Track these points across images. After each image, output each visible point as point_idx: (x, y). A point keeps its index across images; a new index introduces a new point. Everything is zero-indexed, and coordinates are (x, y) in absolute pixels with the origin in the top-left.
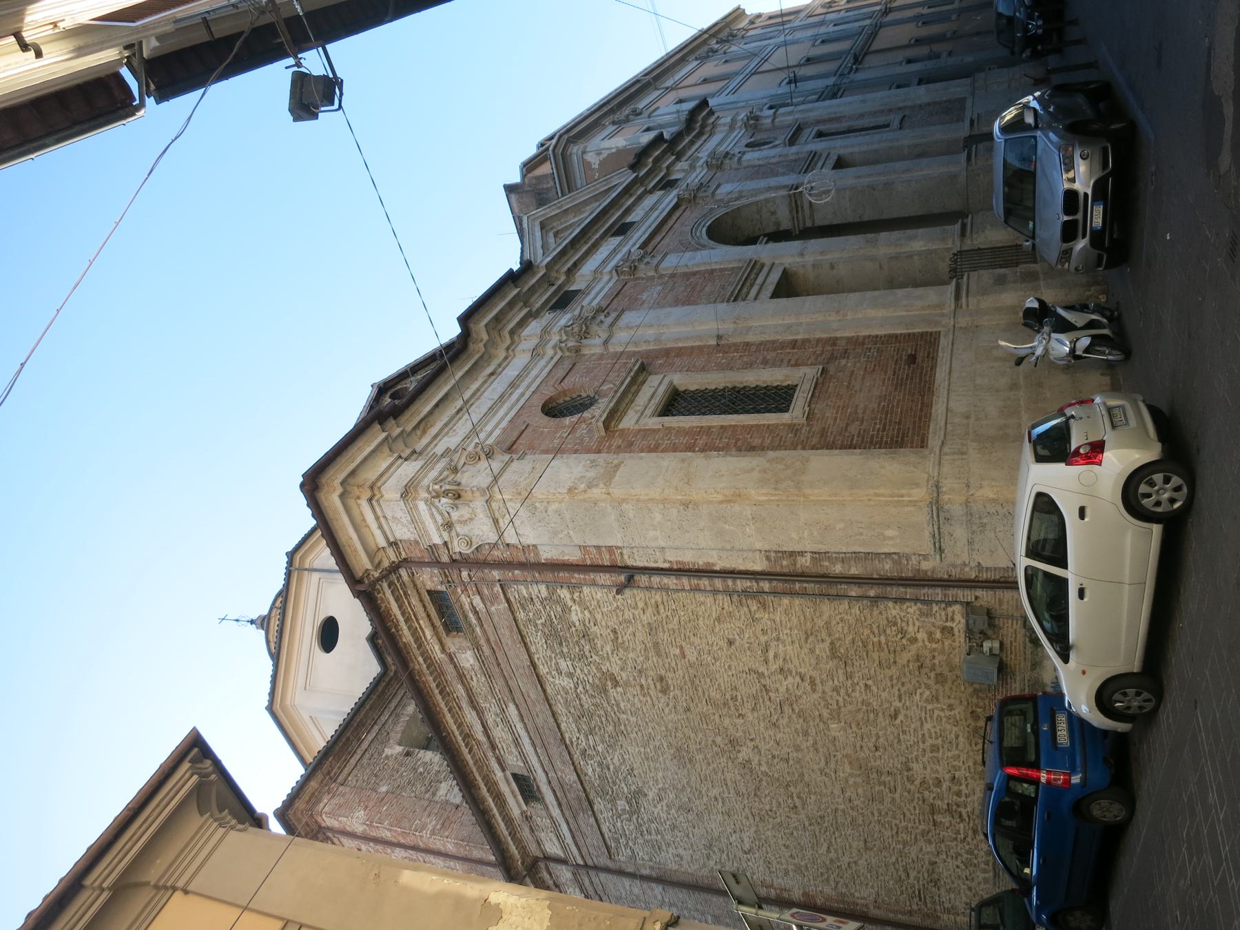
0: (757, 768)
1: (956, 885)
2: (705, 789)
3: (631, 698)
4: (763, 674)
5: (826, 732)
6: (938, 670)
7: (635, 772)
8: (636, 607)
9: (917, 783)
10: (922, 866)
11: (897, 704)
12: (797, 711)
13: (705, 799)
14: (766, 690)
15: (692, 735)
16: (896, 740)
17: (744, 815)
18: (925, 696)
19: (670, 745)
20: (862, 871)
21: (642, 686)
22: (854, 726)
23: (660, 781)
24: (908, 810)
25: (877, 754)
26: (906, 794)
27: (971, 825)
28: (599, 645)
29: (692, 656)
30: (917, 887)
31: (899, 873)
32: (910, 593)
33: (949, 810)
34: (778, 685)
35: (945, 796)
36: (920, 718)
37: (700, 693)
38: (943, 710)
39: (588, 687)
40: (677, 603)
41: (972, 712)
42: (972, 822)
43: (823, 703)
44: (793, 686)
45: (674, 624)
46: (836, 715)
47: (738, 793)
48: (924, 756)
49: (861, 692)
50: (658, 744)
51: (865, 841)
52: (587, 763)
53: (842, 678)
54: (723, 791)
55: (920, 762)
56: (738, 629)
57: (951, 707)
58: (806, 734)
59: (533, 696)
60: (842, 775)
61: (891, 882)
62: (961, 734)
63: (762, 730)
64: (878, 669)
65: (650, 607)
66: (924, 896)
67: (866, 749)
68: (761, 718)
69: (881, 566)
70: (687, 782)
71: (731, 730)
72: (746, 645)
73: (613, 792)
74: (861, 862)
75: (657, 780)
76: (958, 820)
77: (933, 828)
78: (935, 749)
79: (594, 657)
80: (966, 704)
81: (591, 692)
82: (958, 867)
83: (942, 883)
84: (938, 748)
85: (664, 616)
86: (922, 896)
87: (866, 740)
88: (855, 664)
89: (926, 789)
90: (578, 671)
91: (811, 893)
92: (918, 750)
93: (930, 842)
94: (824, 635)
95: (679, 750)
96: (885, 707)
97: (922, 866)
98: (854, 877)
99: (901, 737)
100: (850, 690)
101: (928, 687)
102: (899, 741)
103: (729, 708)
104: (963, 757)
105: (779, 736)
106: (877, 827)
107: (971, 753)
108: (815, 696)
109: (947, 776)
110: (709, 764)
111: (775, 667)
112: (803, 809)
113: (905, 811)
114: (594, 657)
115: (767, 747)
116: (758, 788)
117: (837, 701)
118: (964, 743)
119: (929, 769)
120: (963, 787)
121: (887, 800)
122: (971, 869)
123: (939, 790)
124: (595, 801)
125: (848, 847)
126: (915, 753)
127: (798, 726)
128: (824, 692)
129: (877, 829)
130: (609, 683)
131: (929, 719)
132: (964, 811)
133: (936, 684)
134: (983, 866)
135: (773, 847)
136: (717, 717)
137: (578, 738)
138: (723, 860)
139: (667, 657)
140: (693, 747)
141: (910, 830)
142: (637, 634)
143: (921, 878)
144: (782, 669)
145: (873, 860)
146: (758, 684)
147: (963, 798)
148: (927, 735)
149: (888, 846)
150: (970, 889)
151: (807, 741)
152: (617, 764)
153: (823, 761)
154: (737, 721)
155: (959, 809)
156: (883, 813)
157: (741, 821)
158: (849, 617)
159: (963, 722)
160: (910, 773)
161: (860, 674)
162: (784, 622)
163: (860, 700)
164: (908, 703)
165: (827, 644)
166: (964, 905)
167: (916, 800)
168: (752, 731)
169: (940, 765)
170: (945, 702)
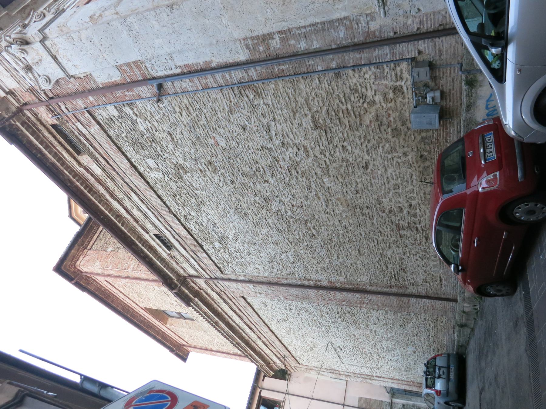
0: (285, 214)
1: (417, 270)
2: (259, 230)
3: (197, 179)
4: (271, 149)
5: (322, 184)
6: (394, 126)
7: (217, 225)
9: (387, 211)
10: (395, 262)
11: (367, 157)
12: (300, 173)
13: (261, 236)
14: (276, 160)
15: (241, 198)
16: (369, 184)
17: (285, 243)
18: (386, 148)
19: (231, 207)
20: (359, 267)
21: (201, 170)
24: (383, 229)
25: (358, 195)
26: (380, 219)
27: (424, 235)
28: (165, 146)
29: (222, 143)
30: (393, 273)
31: (382, 267)
32: (364, 56)
33: (409, 227)
34: (283, 156)
35: (406, 218)
36: (384, 166)
37: (236, 169)
38: (399, 157)
39: (170, 176)
40: (199, 103)
41: (421, 156)
42: (424, 232)
43: (316, 165)
44: (293, 155)
45: (203, 122)
46: (326, 171)
47: (278, 230)
48: (389, 193)
49: (340, 152)
51: (359, 251)
52: (190, 223)
53: (326, 143)
54: (269, 230)
55: (387, 197)
56: (245, 117)
57: (405, 154)
58: (310, 188)
59: (143, 187)
60: (337, 212)
61: (378, 272)
62: (413, 173)
63: (282, 189)
64: (349, 131)
65: (183, 110)
66: (398, 278)
67: (350, 193)
68: (279, 181)
69: (336, 34)
70: (248, 228)
71: (263, 192)
72: (255, 129)
73: (210, 238)
74: (358, 262)
75: (231, 228)
76: (416, 232)
78: (397, 187)
79: (166, 155)
80: (415, 150)
81: (173, 178)
82: (417, 260)
83: (408, 270)
84: (399, 187)
85: (195, 115)
86: (397, 277)
87: (349, 186)
88: (332, 130)
89: (393, 215)
90: (160, 166)
91: (333, 281)
92: (385, 189)
93: (398, 247)
95: (237, 208)
96: (358, 161)
97: (395, 262)
98: (355, 271)
99: (373, 182)
100: (332, 153)
101: (387, 140)
102: (372, 184)
103: (257, 177)
104: (417, 189)
105: (293, 191)
106: (365, 242)
107: (422, 187)
108: (310, 160)
109: (406, 205)
111: (277, 142)
112: (318, 235)
113: (381, 229)
114: (166, 155)
115: (288, 200)
116: (289, 226)
117: (325, 161)
118: (417, 180)
119: (393, 201)
120: (418, 211)
121: (369, 224)
122: (426, 261)
123: (401, 215)
124: (203, 244)
125: (349, 255)
126: (383, 192)
127: (304, 183)
128: (315, 156)
129: (365, 243)
130: (181, 171)
131: (390, 166)
132: (419, 226)
133: (393, 137)
134: (432, 258)
135: (306, 259)
136: (251, 183)
137: (179, 209)
138: (281, 269)
139: (208, 147)
140: (244, 206)
141: (385, 241)
142: (183, 133)
143: (395, 268)
144: (283, 143)
145: (365, 261)
146: (270, 157)
147: (419, 218)
148: (390, 178)
149: (373, 252)
150: (425, 272)
151: (311, 192)
152: (206, 222)
153: (324, 204)
155: (416, 226)
156: (367, 233)
157: (285, 247)
158: (321, 92)
159: (415, 165)
160: (382, 205)
161: (337, 138)
162: (275, 105)
163: (341, 158)
164: (374, 156)
165: (309, 117)
166: (422, 281)
167: (387, 223)
168: (275, 191)
169: (401, 198)
170: (400, 151)
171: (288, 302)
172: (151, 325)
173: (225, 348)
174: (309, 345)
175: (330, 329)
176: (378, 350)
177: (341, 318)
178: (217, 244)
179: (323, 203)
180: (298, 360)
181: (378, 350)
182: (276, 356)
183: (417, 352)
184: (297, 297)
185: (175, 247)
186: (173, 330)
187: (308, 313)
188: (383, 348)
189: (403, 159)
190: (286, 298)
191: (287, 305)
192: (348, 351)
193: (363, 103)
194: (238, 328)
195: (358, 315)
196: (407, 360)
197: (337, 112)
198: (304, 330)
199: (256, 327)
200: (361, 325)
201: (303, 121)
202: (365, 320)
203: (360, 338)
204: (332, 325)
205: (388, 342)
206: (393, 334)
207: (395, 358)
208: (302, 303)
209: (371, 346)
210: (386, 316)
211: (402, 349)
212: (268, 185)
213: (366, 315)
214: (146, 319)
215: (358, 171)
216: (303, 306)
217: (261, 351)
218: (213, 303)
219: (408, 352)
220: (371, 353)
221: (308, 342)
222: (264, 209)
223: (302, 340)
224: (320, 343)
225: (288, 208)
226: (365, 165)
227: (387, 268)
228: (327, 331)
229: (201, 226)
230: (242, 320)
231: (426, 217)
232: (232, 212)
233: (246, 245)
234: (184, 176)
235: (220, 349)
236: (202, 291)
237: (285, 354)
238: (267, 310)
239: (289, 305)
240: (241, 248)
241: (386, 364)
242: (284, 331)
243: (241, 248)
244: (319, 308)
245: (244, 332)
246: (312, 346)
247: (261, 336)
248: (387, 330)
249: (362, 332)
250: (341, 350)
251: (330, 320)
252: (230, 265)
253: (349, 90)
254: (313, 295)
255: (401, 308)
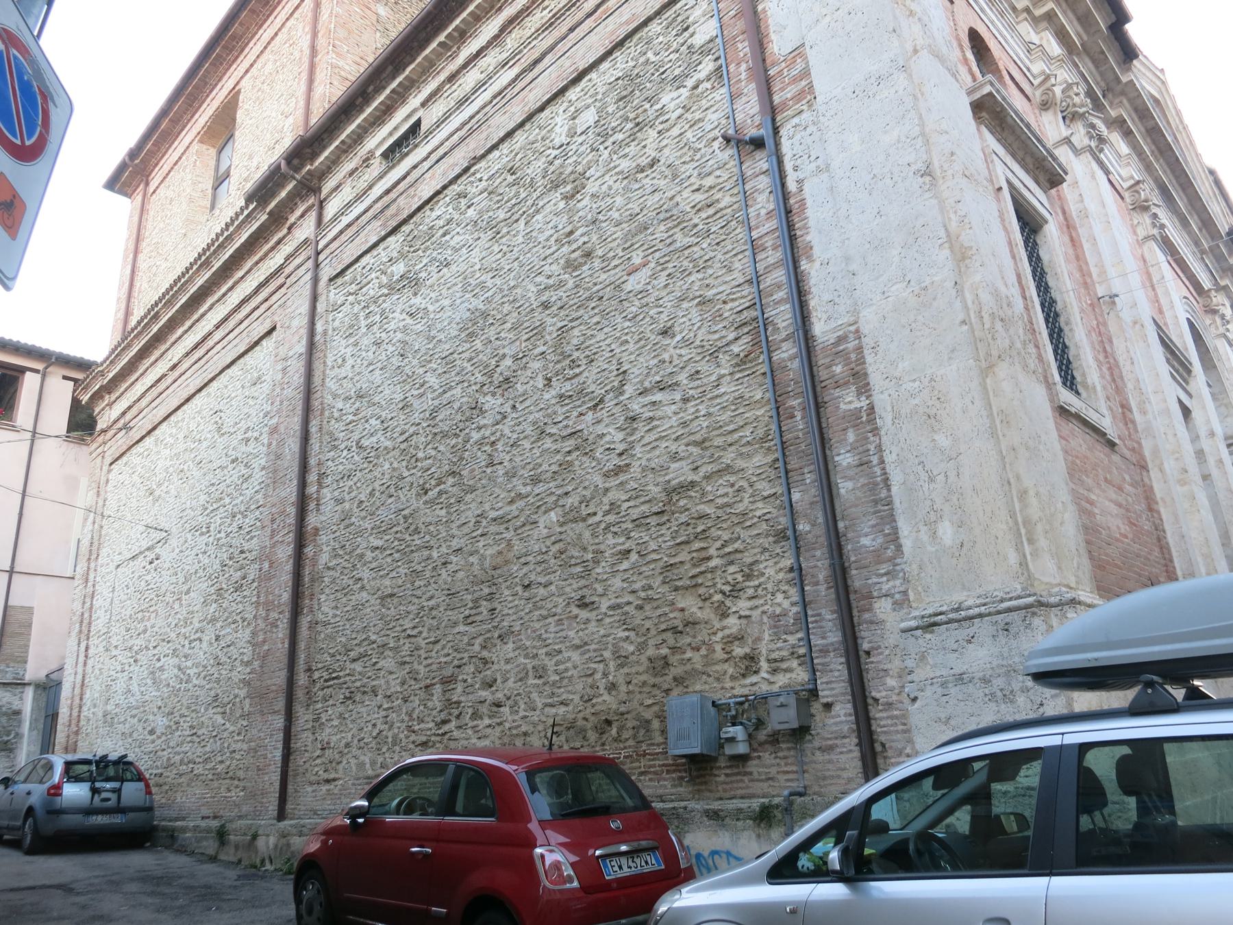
0: (473, 426)
2: (435, 366)
3: (551, 225)
4: (621, 394)
5: (543, 508)
6: (673, 659)
7: (445, 270)
8: (701, 176)
9: (485, 654)
10: (369, 678)
11: (604, 605)
12: (568, 458)
13: (421, 371)
14: (597, 405)
15: (508, 325)
16: (544, 613)
17: (407, 427)
18: (625, 645)
19: (488, 301)
20: (353, 597)
21: (571, 233)
22: (557, 546)
23: (437, 305)
24: (443, 647)
25: (519, 589)
26: (466, 639)
28: (627, 150)
29: (633, 283)
30: (341, 674)
31: (356, 648)
33: (449, 704)
34: (607, 421)
35: (470, 697)
36: (586, 644)
37: (574, 315)
38: (605, 675)
39: (557, 162)
40: (721, 231)
41: (608, 723)
42: (438, 738)
43: (587, 493)
44: (608, 443)
45: (681, 240)
46: (572, 517)
47: (435, 410)
48: (526, 656)
49: (615, 545)
50: (489, 284)
51: (392, 595)
52: (448, 205)
53: (635, 513)
54: (435, 391)
55: (516, 653)
56: (692, 335)
57: (612, 687)
58: (535, 480)
59: (531, 97)
60: (481, 544)
61: (343, 639)
62: (571, 708)
63: (531, 418)
64: (661, 564)
65: (706, 195)
66: (331, 686)
68: (549, 411)
69: (867, 530)
70: (440, 341)
71: (524, 376)
72: (666, 356)
73: (414, 252)
74: (364, 594)
75: (438, 301)
76: (438, 719)
77: (422, 684)
78: (540, 673)
79: (606, 152)
80: (622, 709)
81: (552, 168)
82: (374, 725)
84: (541, 677)
85: (696, 221)
86: (332, 683)
87: (539, 569)
88: (664, 527)
89: (477, 667)
90: (580, 140)
91: (318, 538)
92: (534, 647)
93: (403, 683)
94: (706, 469)
95: (485, 315)
96: (597, 586)
97: (369, 678)
98: (344, 589)
99: (550, 620)
101: (642, 647)
102: (546, 618)
103: (559, 362)
104: (535, 716)
105: (527, 444)
106: (413, 608)
107: (540, 728)
108: (598, 480)
109: (500, 695)
110: (470, 359)
111: (636, 407)
112: (426, 503)
114: (606, 152)
115: (507, 431)
116: (445, 435)
117: (595, 514)
118: (557, 714)
119: (508, 667)
120: (487, 721)
121: (454, 615)
122: (373, 745)
123: (477, 686)
124: (399, 235)
125: (381, 573)
126: (528, 643)
127: (545, 467)
128: (607, 490)
129: (411, 608)
130: (569, 188)
131: (587, 656)
133: (650, 659)
134: (380, 759)
135: (369, 476)
136: (543, 349)
137: (480, 180)
138: (344, 418)
139: (624, 249)
140: (491, 333)
141: (416, 652)
142: (656, 194)
143: (353, 678)
144: (633, 419)
145: (369, 610)
146: (603, 391)
148: (560, 657)
149: (391, 626)
150: (347, 745)
151: (525, 485)
152: (452, 243)
153: (497, 513)
154: (540, 377)
155: (453, 719)
156: (434, 613)
157: (396, 427)
158: (746, 501)
159: (590, 710)
161: (647, 538)
162: (718, 401)
163: (602, 547)
164: (608, 620)
165: (691, 477)
166: (326, 740)
167: (459, 656)
168: (527, 403)
169: (515, 682)
171: (265, 436)
172: (196, 104)
173: (145, 285)
174: (160, 485)
175: (202, 534)
176: (155, 647)
177: (231, 559)
178: (399, 269)
179: (500, 512)
180: (119, 462)
181: (155, 647)
182: (130, 408)
183: (154, 736)
184: (278, 457)
185: (391, 168)
186: (184, 158)
187: (239, 482)
188: (159, 660)
189: (602, 684)
190: (274, 430)
191: (256, 434)
192: (148, 578)
193: (723, 593)
194: (195, 317)
195: (239, 599)
196: (133, 716)
197: (703, 535)
198: (197, 473)
199: (200, 359)
200: (214, 605)
201: (683, 463)
202: (226, 614)
203: (181, 605)
204: (211, 539)
205: (176, 671)
206: (195, 681)
207: (135, 688)
208: (263, 468)
209: (163, 630)
210: (237, 663)
211: (159, 703)
212: (541, 386)
213: (238, 618)
214: (211, 92)
215: (575, 586)
216: (256, 470)
217: (141, 371)
218: (256, 258)
219: (151, 717)
220: (145, 631)
221: (166, 484)
222: (485, 378)
223: (171, 470)
224: (165, 511)
225: (487, 433)
226: (587, 600)
227: (354, 660)
228: (195, 529)
229: (441, 232)
230: (217, 327)
231: (474, 741)
232: (478, 303)
233: (399, 335)
234: (558, 194)
235: (140, 274)
236: (285, 231)
237: (134, 430)
238: (243, 387)
239: (256, 439)
240: (392, 326)
241: (119, 668)
242: (193, 426)
243: (392, 326)
244: (253, 507)
245: (186, 331)
246: (157, 493)
247: (176, 373)
248: (204, 667)
249: (196, 609)
250: (151, 563)
251: (223, 535)
252: (351, 298)
253: (749, 560)
254: (283, 494)
255: (258, 695)
